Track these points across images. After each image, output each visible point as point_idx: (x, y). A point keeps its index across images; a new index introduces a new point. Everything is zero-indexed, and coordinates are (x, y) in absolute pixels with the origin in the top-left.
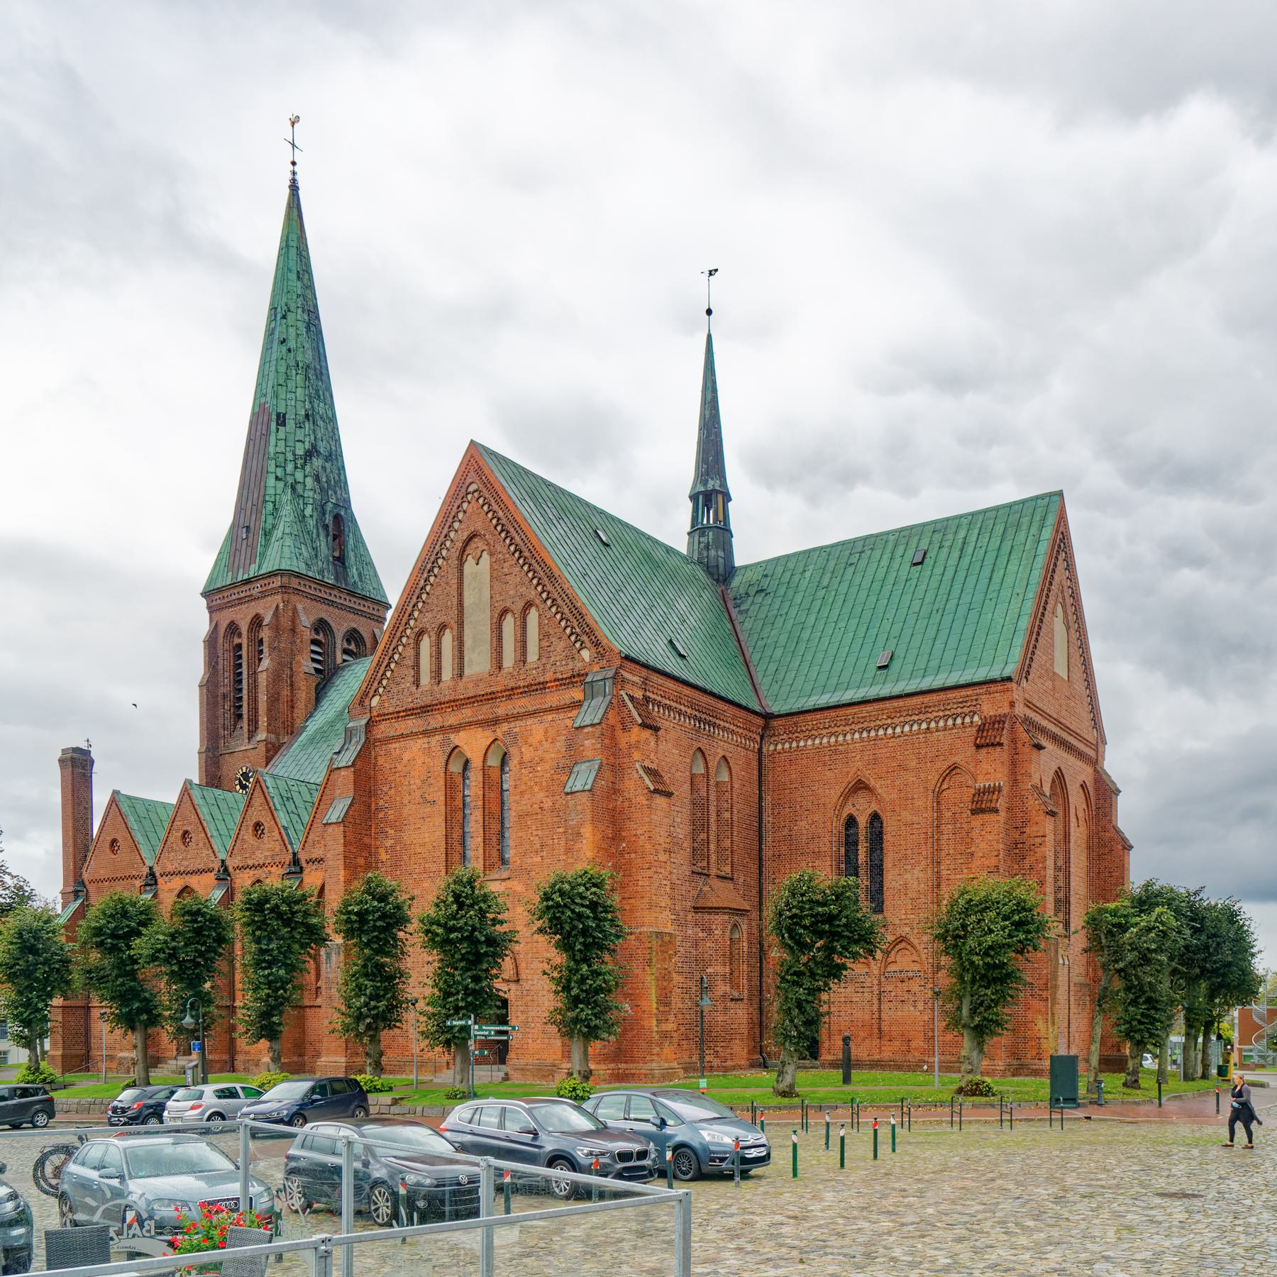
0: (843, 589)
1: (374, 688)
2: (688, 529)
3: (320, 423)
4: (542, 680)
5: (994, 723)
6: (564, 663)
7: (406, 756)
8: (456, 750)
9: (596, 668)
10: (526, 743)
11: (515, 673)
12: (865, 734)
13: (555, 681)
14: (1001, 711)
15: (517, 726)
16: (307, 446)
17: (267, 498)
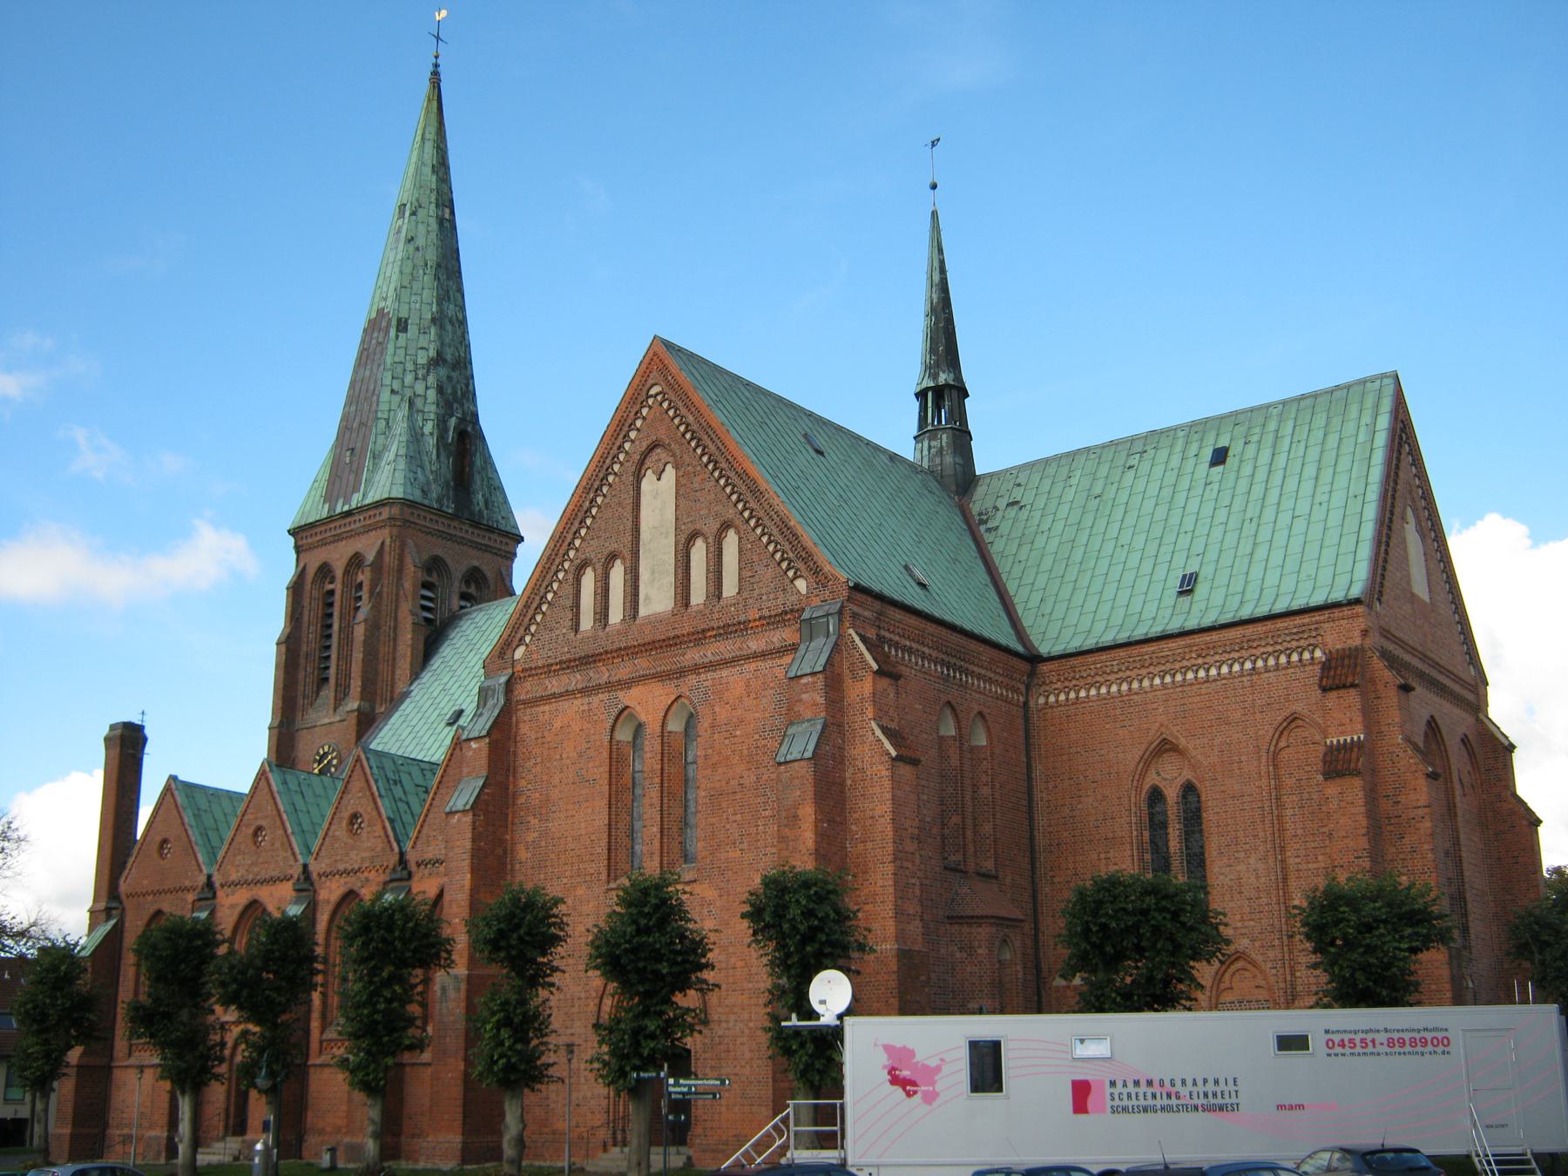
0: (1123, 497)
1: (519, 636)
2: (915, 432)
3: (449, 328)
4: (742, 618)
5: (1343, 659)
6: (772, 596)
8: (626, 713)
9: (816, 601)
11: (707, 612)
12: (1168, 679)
16: (432, 353)
17: (379, 415)
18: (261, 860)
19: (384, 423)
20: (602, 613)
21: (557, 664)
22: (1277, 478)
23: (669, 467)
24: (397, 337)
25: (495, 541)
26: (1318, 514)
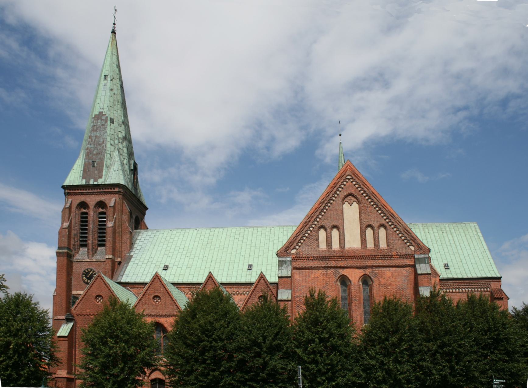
4: (390, 254)
10: (382, 277)
13: (397, 255)
15: (377, 270)
16: (124, 135)
18: (158, 308)
19: (109, 155)
20: (329, 243)
21: (311, 257)
22: (457, 243)
24: (111, 125)
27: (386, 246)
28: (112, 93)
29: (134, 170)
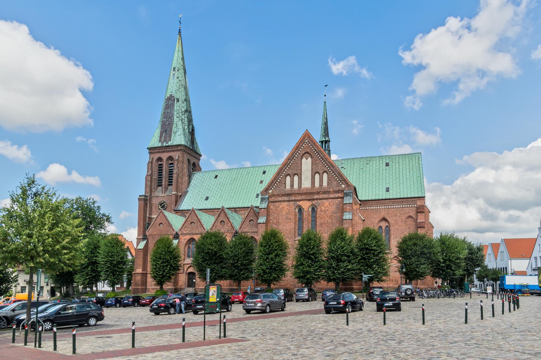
0: (368, 170)
1: (270, 188)
3: (188, 102)
4: (329, 190)
7: (281, 207)
10: (323, 205)
14: (422, 204)
15: (319, 201)
17: (174, 122)
20: (292, 185)
22: (401, 171)
23: (309, 158)
25: (197, 156)
26: (412, 179)
27: (327, 185)
28: (178, 80)
29: (192, 133)
